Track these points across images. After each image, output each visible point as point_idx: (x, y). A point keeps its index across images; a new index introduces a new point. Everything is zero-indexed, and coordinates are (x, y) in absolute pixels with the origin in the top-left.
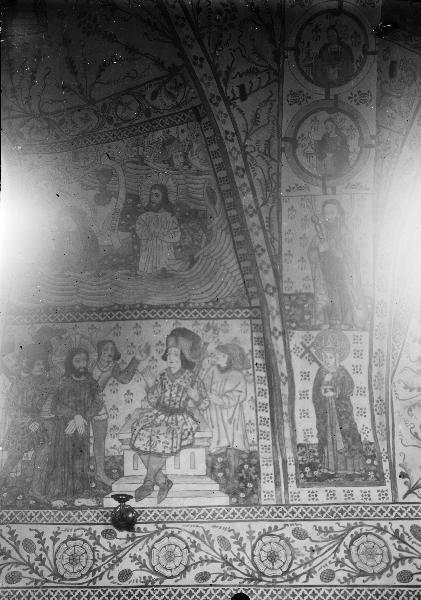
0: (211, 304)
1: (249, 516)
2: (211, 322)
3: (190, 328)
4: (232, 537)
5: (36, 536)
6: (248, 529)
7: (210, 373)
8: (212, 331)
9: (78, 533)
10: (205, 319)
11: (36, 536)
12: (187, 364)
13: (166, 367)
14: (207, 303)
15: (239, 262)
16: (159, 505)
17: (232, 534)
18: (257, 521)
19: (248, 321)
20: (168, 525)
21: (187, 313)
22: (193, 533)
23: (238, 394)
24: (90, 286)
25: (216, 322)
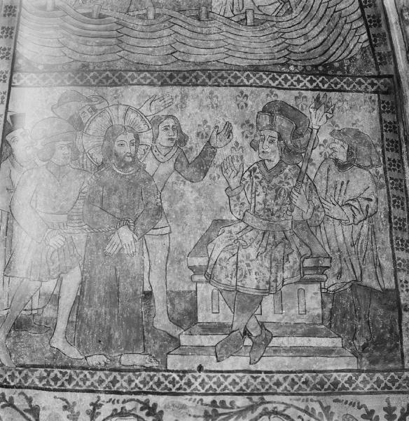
0: (320, 68)
1: (386, 386)
2: (322, 94)
3: (292, 103)
4: (363, 416)
5: (65, 408)
6: (386, 405)
7: (324, 169)
8: (323, 107)
9: (129, 406)
10: (312, 90)
11: (65, 408)
12: (289, 152)
13: (256, 159)
14: (316, 66)
15: (361, 7)
16: (252, 368)
17: (363, 411)
18: (399, 393)
19: (375, 97)
20: (267, 398)
21: (286, 80)
22: (306, 411)
23: (366, 203)
24: (142, 35)
25: (332, 94)
